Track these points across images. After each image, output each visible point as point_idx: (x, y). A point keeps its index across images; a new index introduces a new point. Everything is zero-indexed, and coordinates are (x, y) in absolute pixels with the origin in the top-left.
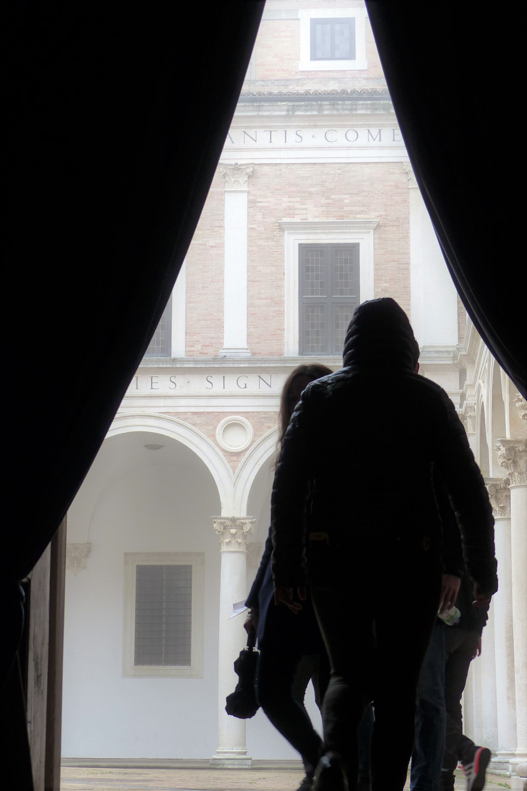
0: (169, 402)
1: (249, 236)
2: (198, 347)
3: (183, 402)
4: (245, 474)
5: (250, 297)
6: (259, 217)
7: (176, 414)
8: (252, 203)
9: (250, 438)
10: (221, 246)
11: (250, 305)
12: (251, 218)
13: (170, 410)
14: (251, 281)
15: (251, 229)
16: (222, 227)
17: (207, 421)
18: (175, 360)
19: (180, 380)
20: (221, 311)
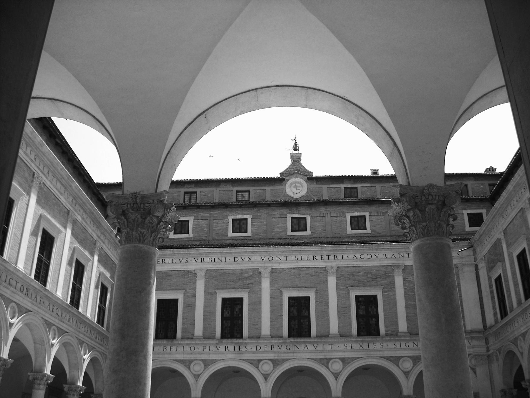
0: (381, 353)
1: (405, 291)
2: (390, 332)
3: (386, 352)
4: (411, 379)
5: (407, 313)
6: (407, 284)
7: (384, 357)
8: (404, 279)
9: (412, 366)
10: (395, 295)
11: (407, 316)
12: (404, 284)
13: (382, 356)
14: (407, 307)
15: (404, 289)
16: (394, 288)
17: (396, 360)
18: (382, 337)
19: (384, 344)
20: (397, 318)
